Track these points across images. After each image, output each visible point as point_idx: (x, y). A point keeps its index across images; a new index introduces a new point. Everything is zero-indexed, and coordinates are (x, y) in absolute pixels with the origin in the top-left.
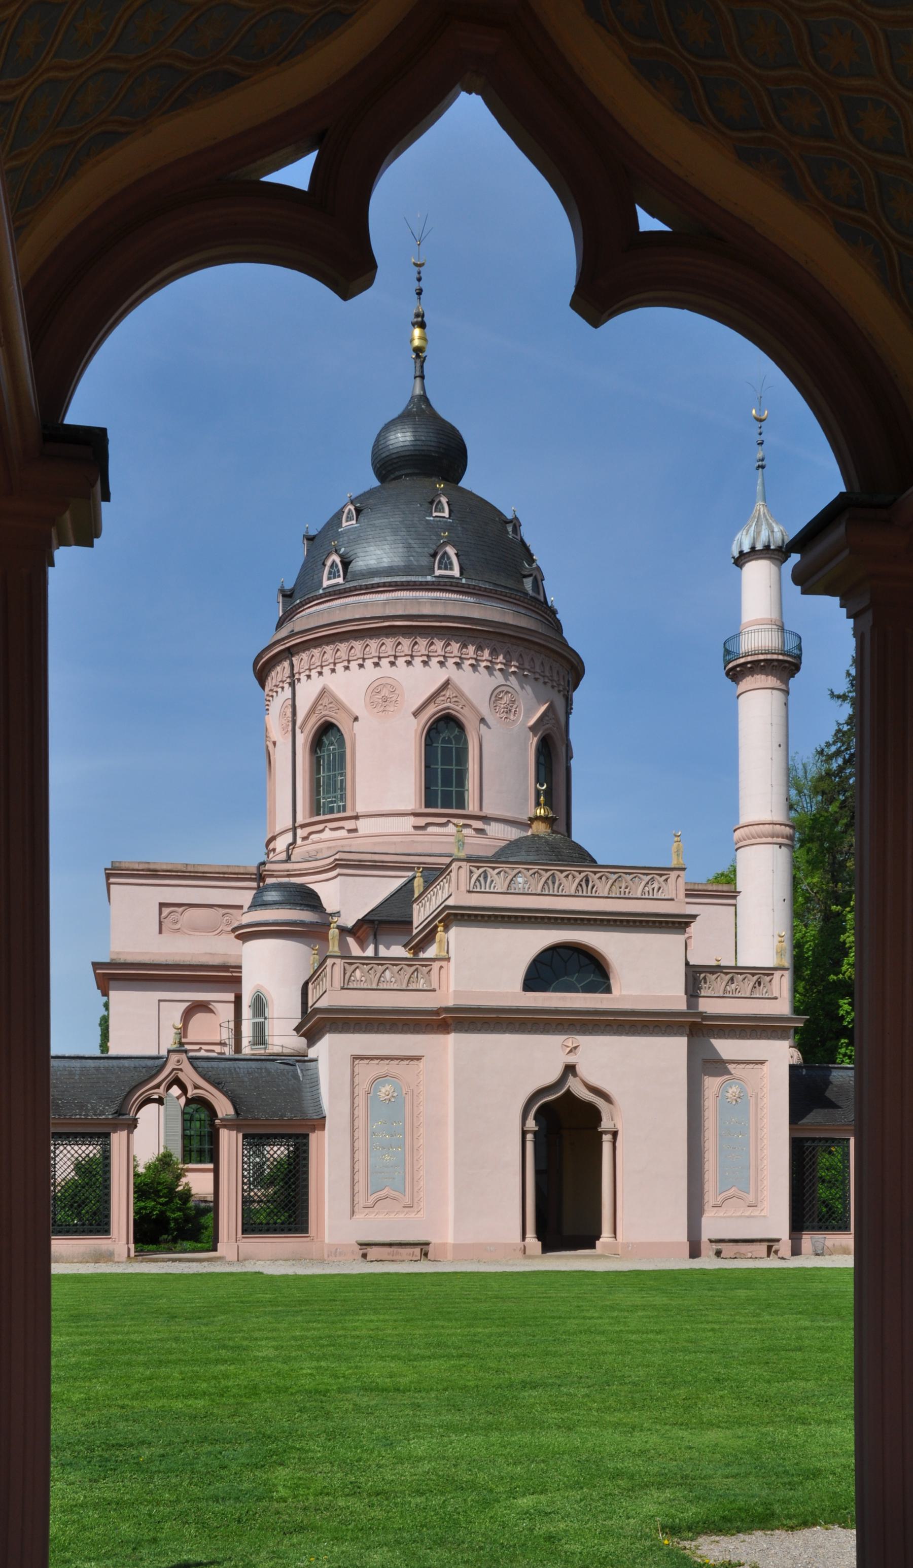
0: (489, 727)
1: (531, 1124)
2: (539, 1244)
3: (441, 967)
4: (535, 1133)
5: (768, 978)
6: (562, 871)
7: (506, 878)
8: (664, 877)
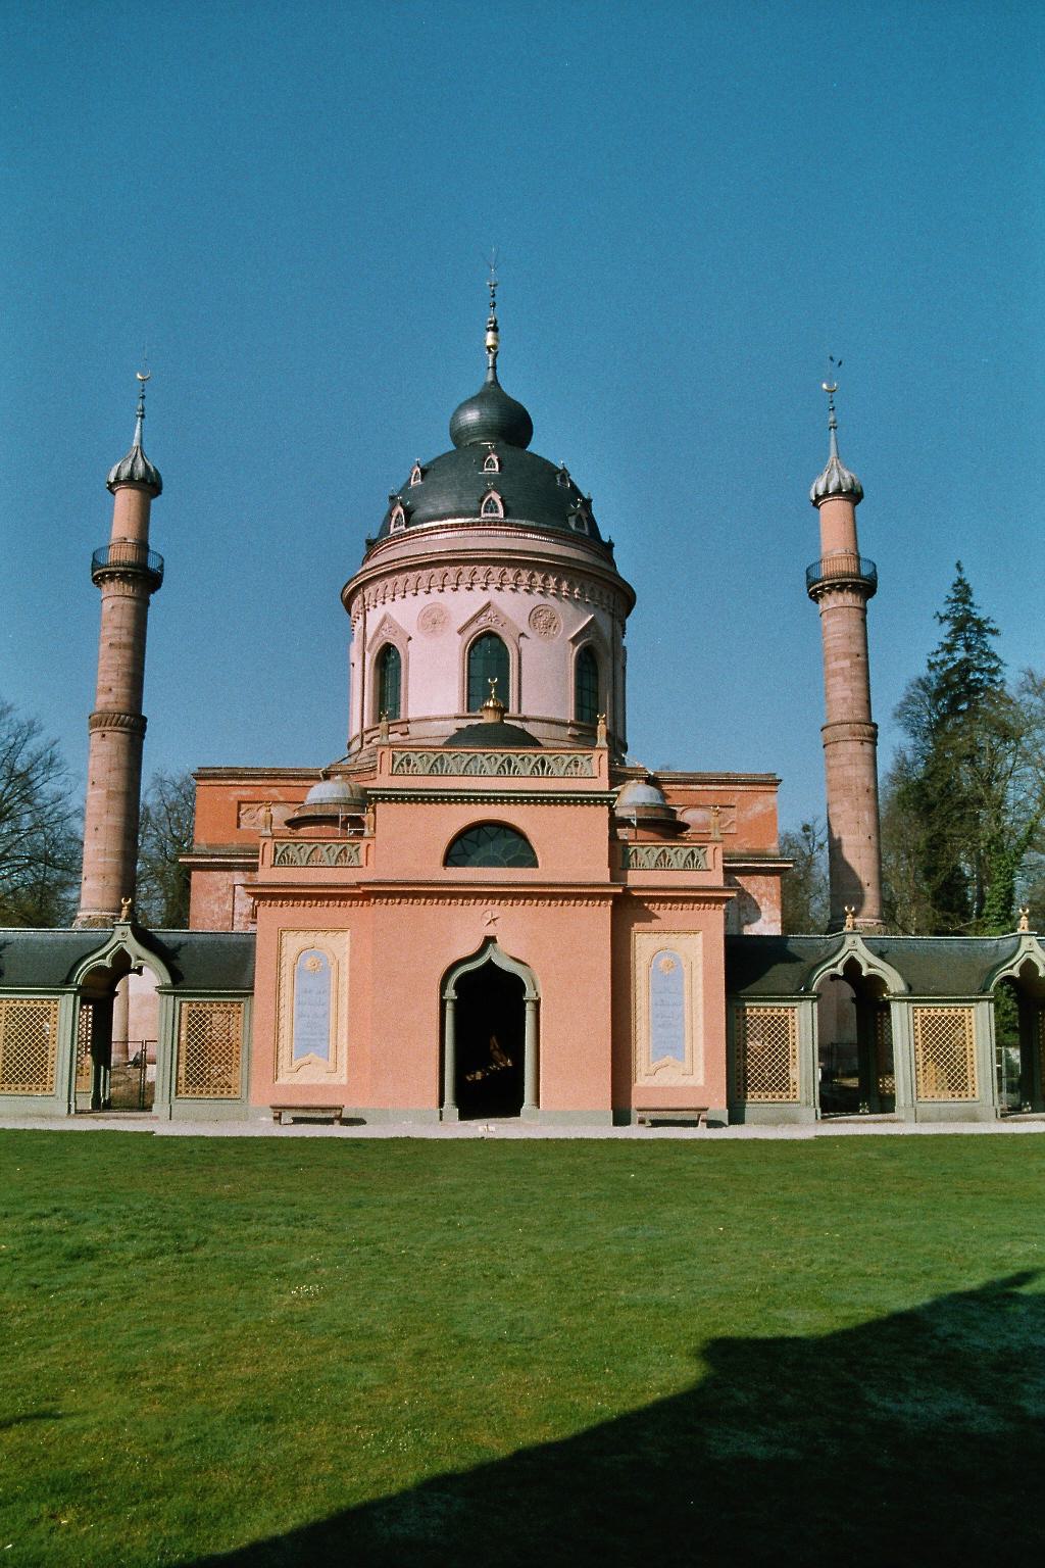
0: (528, 638)
1: (451, 993)
8: (587, 757)
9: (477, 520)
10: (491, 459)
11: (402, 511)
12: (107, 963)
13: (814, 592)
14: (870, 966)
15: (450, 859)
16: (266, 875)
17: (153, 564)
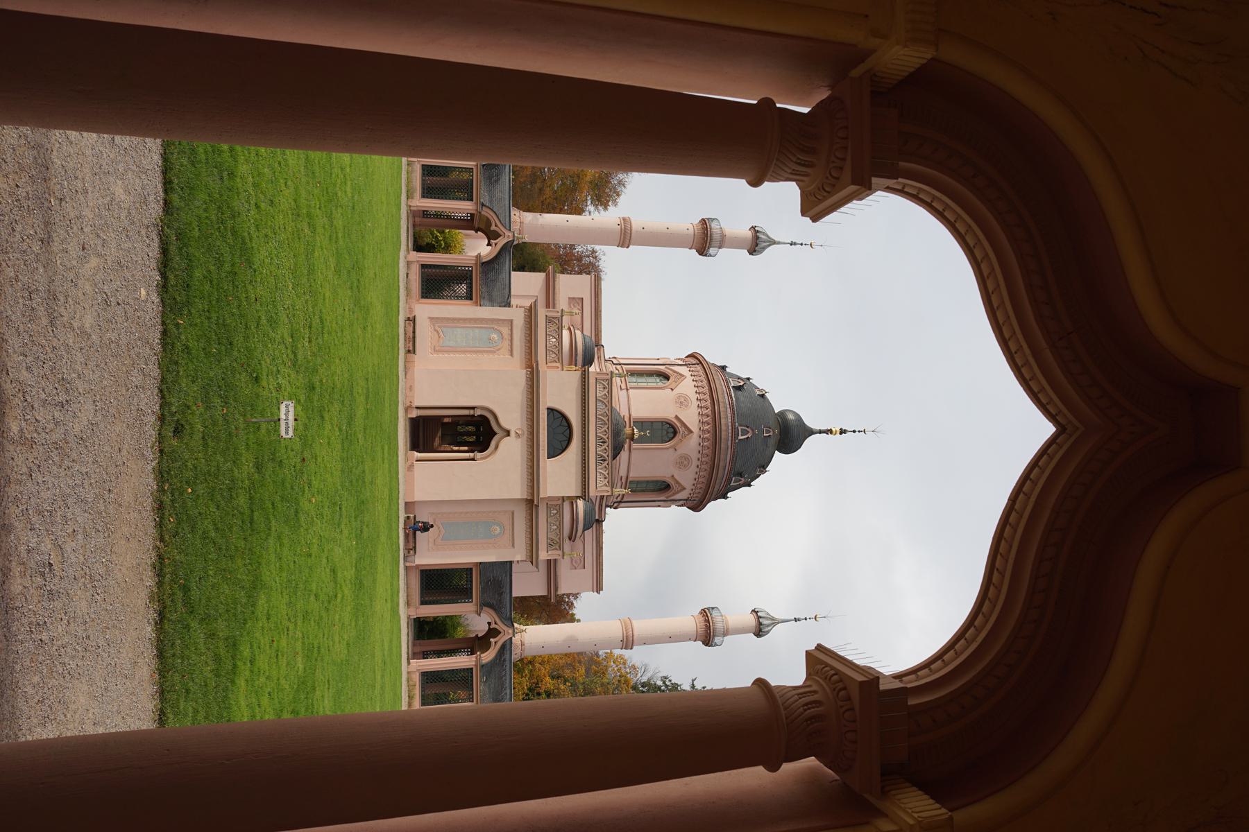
1: (478, 413)
2: (414, 416)
3: (558, 367)
4: (473, 416)
5: (558, 548)
6: (608, 428)
7: (604, 399)
9: (737, 424)
10: (770, 432)
11: (741, 384)
12: (493, 228)
13: (705, 612)
14: (495, 643)
15: (551, 411)
16: (542, 313)
17: (712, 251)
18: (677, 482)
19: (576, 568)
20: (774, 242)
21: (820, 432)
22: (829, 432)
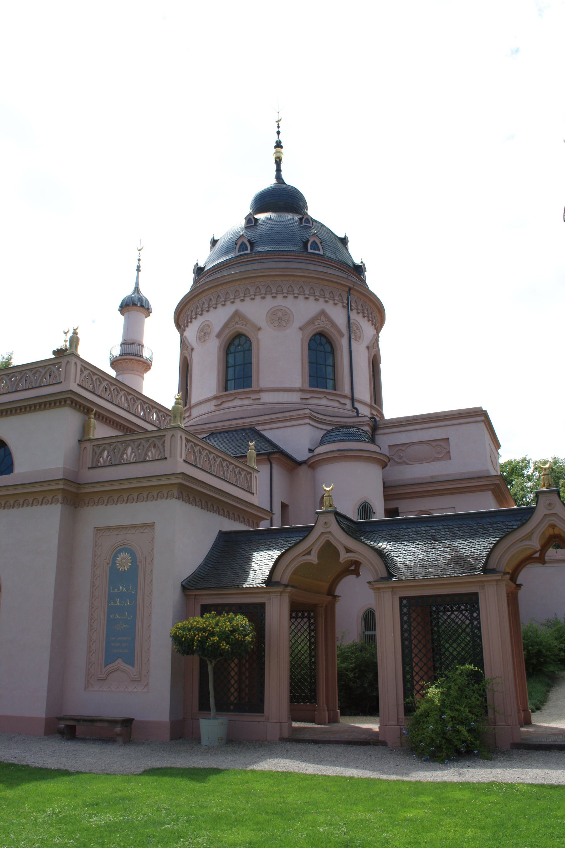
18: (311, 322)
19: (449, 452)
20: (137, 289)
21: (279, 170)
22: (278, 162)
